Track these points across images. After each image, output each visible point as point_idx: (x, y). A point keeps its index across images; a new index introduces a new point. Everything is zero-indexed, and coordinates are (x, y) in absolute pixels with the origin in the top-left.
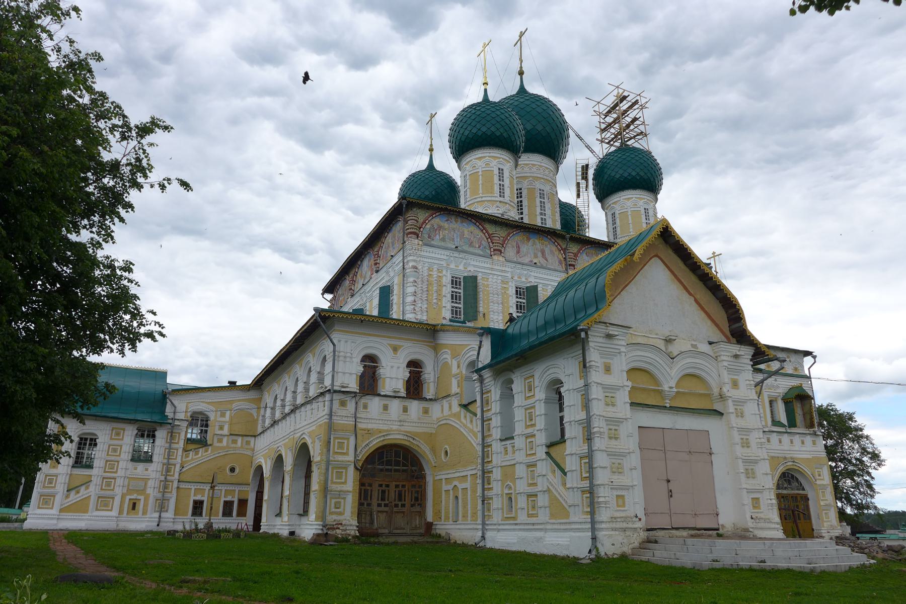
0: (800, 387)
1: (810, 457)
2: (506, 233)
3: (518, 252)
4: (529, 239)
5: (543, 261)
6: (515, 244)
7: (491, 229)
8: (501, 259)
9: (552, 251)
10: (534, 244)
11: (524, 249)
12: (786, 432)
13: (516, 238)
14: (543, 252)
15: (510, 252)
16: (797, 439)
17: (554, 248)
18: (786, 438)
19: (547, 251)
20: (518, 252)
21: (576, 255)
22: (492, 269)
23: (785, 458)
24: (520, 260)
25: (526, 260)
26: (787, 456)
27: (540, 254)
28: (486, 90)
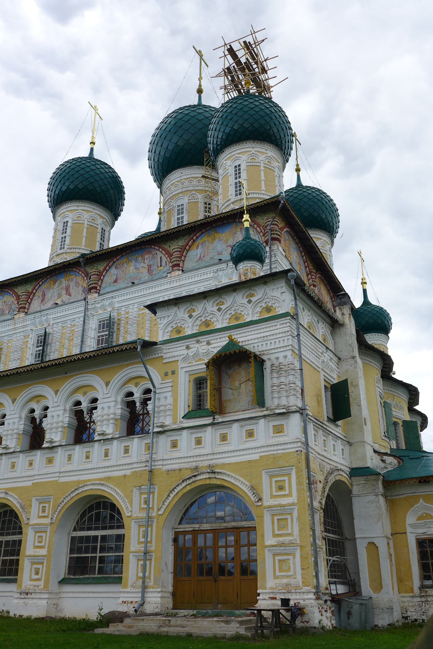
0: (232, 343)
1: (256, 457)
2: (32, 288)
3: (42, 301)
4: (55, 282)
5: (65, 298)
6: (40, 294)
7: (20, 290)
8: (22, 315)
9: (77, 284)
10: (60, 284)
11: (49, 295)
12: (212, 424)
13: (43, 287)
14: (67, 289)
15: (35, 305)
16: (235, 432)
17: (79, 279)
18: (209, 435)
19: (72, 284)
20: (42, 301)
21: (100, 275)
22: (15, 329)
23: (196, 468)
24: (43, 308)
25: (50, 304)
26: (201, 464)
27: (64, 292)
28: (92, 149)
